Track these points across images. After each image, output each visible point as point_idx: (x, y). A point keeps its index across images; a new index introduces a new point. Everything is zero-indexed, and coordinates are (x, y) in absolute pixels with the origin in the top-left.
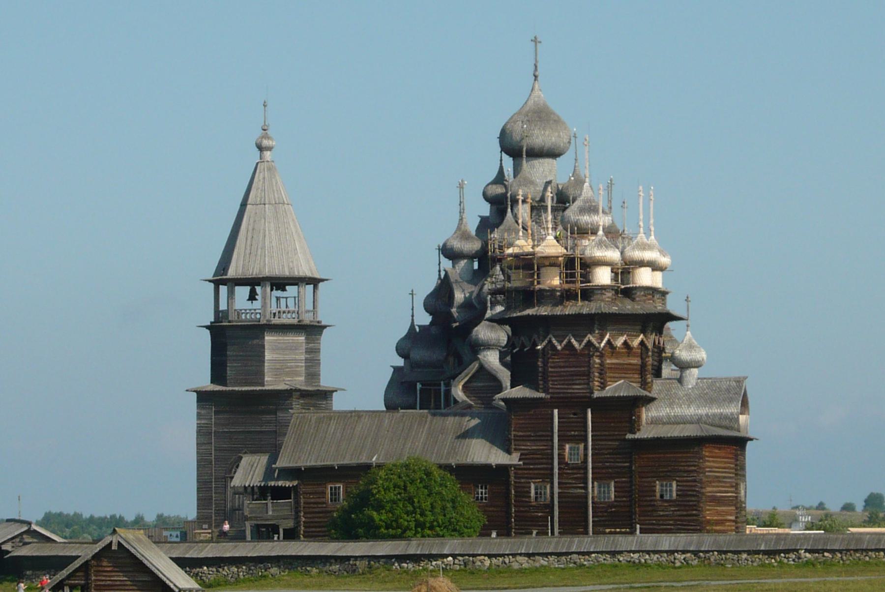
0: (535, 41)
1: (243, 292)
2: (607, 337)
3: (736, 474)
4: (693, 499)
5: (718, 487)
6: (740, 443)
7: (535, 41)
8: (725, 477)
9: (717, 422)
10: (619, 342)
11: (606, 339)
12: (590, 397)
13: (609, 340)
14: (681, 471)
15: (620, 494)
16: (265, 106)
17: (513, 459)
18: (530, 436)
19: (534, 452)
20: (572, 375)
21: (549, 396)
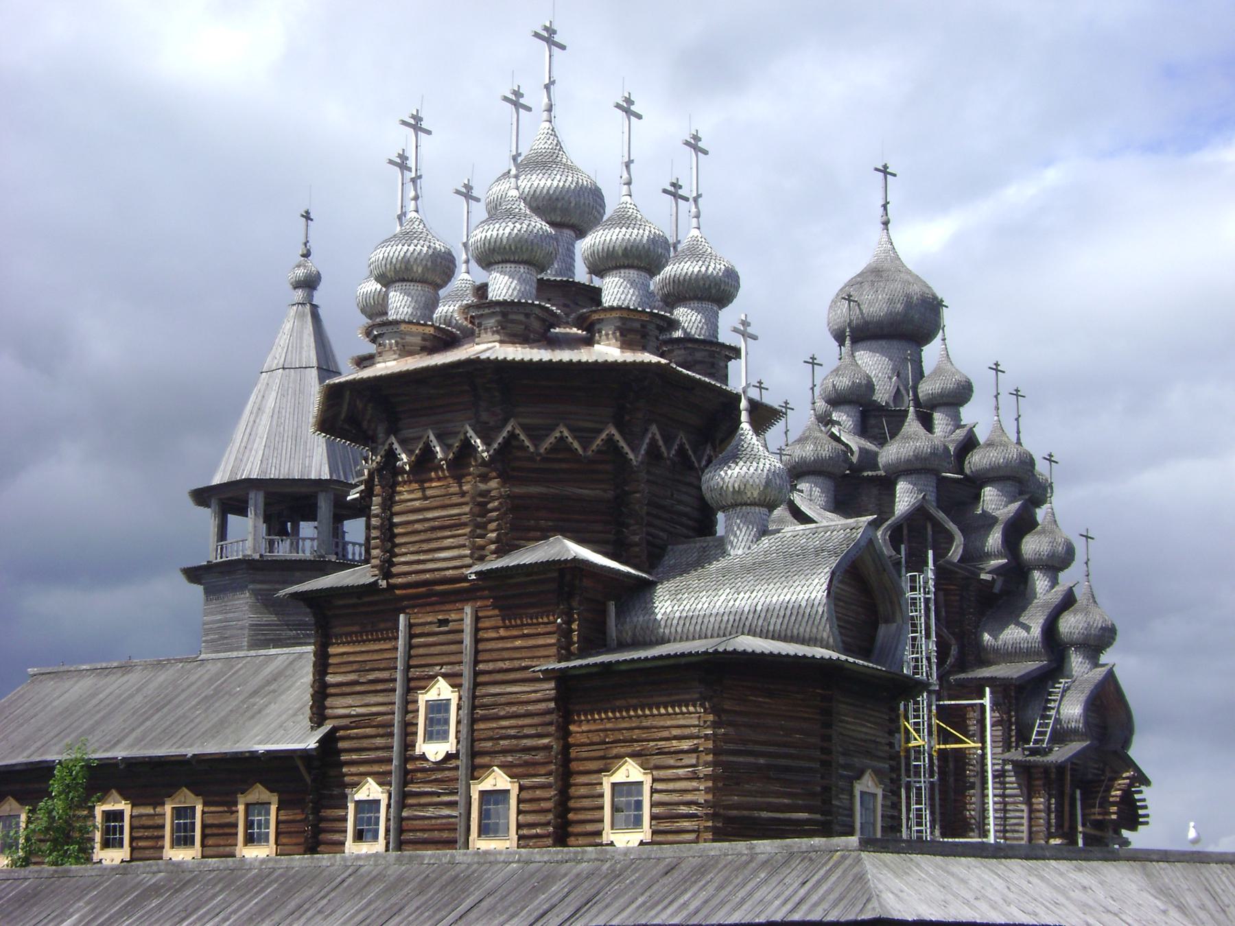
0: (885, 171)
2: (509, 428)
3: (825, 764)
4: (686, 824)
5: (764, 794)
7: (885, 171)
8: (787, 769)
9: (775, 624)
10: (552, 440)
11: (505, 434)
12: (465, 579)
13: (513, 436)
14: (661, 752)
15: (530, 818)
16: (307, 216)
18: (356, 683)
19: (360, 721)
20: (433, 529)
21: (383, 584)
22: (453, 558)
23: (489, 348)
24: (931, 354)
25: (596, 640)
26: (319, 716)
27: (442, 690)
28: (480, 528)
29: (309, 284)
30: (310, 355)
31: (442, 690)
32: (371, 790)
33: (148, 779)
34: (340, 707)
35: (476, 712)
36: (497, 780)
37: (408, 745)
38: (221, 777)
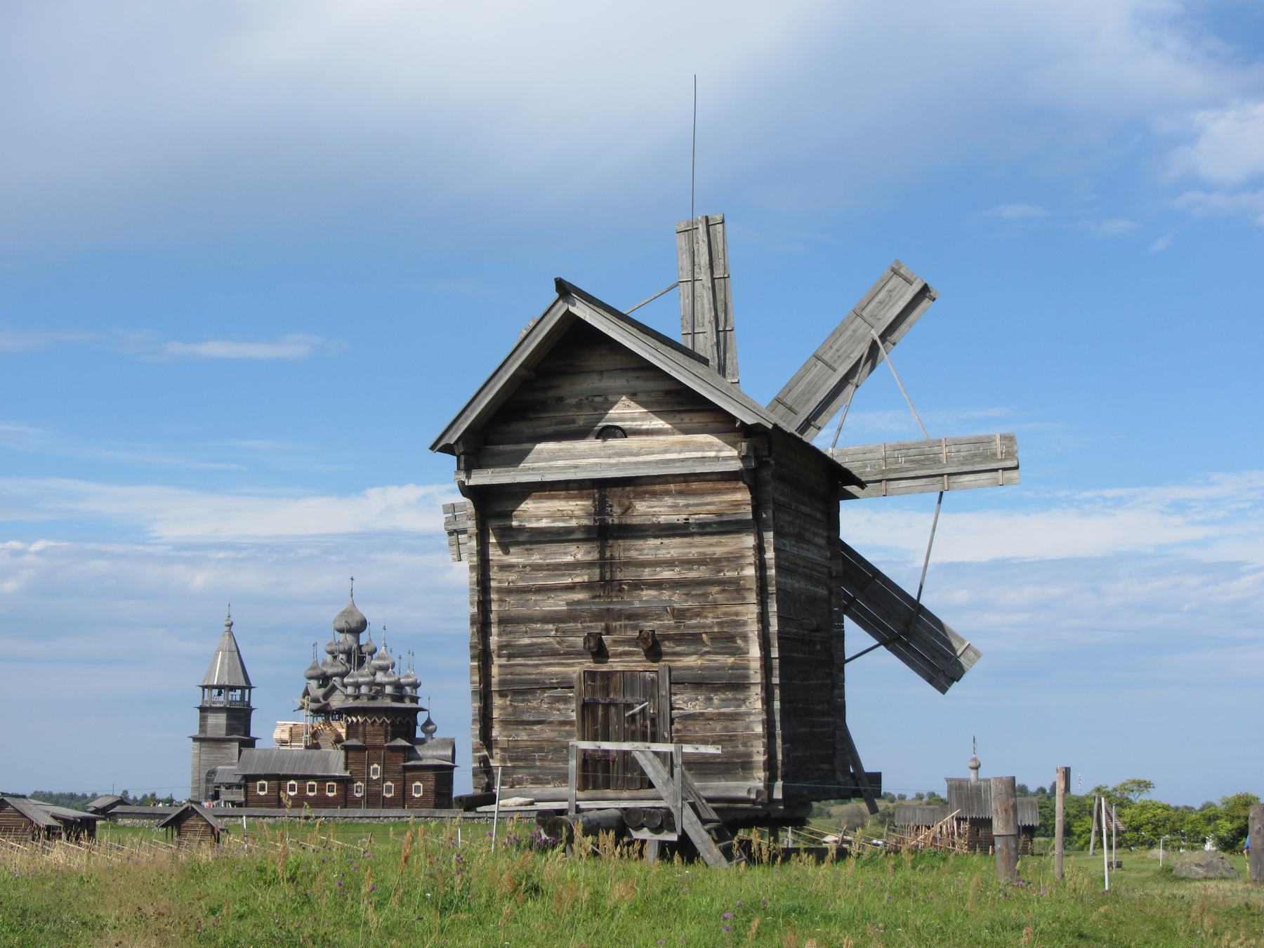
1: (215, 692)
6: (452, 768)
17: (348, 774)
22: (379, 741)
23: (388, 703)
24: (364, 638)
25: (410, 760)
26: (346, 769)
27: (376, 766)
28: (386, 737)
29: (230, 625)
30: (234, 648)
31: (376, 766)
32: (359, 783)
33: (303, 778)
34: (352, 767)
35: (384, 771)
36: (389, 783)
37: (368, 774)
38: (322, 779)
